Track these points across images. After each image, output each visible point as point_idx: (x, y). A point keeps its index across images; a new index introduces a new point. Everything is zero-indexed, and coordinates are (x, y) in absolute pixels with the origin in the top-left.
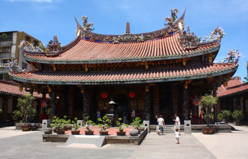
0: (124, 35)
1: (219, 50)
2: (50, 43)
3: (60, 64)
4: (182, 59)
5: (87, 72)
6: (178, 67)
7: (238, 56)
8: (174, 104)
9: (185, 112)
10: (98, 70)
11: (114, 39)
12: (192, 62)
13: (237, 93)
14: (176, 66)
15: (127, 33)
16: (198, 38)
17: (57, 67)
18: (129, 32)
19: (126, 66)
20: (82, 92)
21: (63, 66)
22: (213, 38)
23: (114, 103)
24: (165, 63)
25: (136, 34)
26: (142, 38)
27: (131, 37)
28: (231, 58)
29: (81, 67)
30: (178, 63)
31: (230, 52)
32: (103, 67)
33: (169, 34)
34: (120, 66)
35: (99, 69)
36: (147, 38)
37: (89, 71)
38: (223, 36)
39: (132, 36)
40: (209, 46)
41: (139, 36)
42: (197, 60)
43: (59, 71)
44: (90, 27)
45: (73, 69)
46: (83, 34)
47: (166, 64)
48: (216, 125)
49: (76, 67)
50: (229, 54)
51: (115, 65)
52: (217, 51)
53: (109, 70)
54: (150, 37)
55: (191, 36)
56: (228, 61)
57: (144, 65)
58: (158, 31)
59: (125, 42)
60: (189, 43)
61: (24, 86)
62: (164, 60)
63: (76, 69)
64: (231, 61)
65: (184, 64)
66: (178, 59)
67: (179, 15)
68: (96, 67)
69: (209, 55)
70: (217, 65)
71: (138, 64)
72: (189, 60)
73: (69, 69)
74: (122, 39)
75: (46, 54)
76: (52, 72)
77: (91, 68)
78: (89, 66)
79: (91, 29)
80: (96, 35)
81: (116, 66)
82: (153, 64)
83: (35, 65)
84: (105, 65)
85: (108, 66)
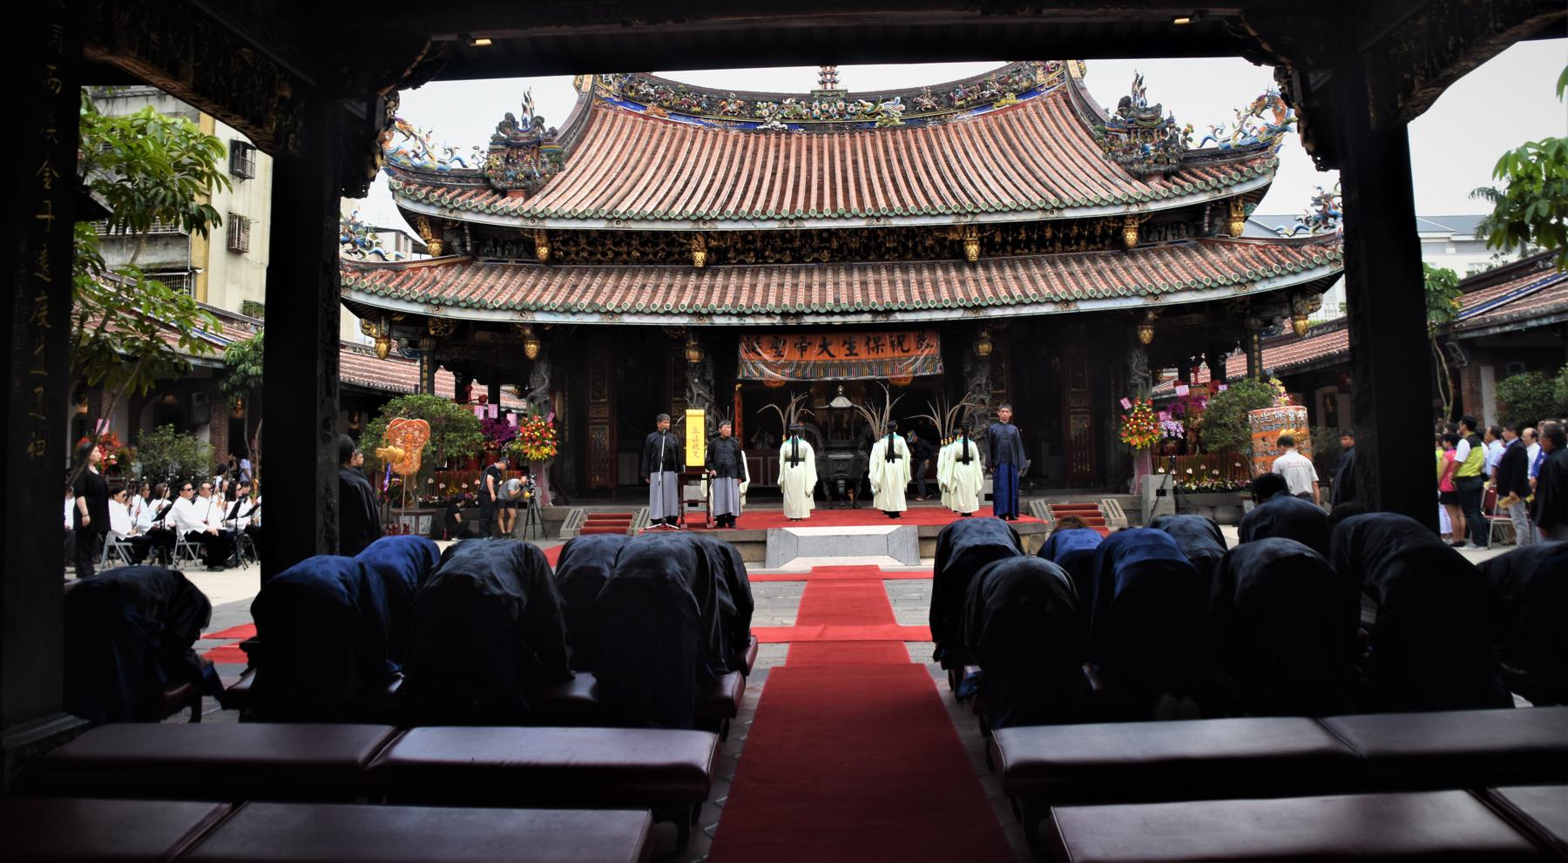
0: (809, 98)
2: (501, 127)
3: (566, 231)
4: (1121, 219)
5: (700, 268)
6: (1103, 253)
8: (1073, 413)
11: (765, 112)
12: (1160, 233)
13: (1314, 362)
14: (1092, 246)
15: (823, 83)
17: (551, 242)
20: (693, 355)
21: (583, 241)
24: (1049, 234)
25: (870, 93)
26: (895, 109)
27: (843, 104)
30: (1104, 235)
31: (1317, 194)
33: (1017, 97)
35: (752, 254)
36: (922, 112)
37: (707, 263)
39: (850, 98)
41: (883, 101)
42: (1178, 223)
43: (559, 261)
45: (629, 254)
47: (1054, 238)
49: (643, 244)
50: (1317, 201)
51: (828, 240)
54: (933, 109)
59: (815, 127)
60: (1144, 149)
61: (395, 334)
64: (1322, 231)
65: (1131, 237)
66: (1106, 218)
68: (739, 245)
70: (1265, 247)
71: (936, 234)
72: (1148, 224)
73: (611, 255)
74: (804, 111)
76: (521, 268)
78: (713, 243)
81: (835, 245)
82: (998, 239)
83: (443, 231)
84: (784, 240)
85: (797, 244)
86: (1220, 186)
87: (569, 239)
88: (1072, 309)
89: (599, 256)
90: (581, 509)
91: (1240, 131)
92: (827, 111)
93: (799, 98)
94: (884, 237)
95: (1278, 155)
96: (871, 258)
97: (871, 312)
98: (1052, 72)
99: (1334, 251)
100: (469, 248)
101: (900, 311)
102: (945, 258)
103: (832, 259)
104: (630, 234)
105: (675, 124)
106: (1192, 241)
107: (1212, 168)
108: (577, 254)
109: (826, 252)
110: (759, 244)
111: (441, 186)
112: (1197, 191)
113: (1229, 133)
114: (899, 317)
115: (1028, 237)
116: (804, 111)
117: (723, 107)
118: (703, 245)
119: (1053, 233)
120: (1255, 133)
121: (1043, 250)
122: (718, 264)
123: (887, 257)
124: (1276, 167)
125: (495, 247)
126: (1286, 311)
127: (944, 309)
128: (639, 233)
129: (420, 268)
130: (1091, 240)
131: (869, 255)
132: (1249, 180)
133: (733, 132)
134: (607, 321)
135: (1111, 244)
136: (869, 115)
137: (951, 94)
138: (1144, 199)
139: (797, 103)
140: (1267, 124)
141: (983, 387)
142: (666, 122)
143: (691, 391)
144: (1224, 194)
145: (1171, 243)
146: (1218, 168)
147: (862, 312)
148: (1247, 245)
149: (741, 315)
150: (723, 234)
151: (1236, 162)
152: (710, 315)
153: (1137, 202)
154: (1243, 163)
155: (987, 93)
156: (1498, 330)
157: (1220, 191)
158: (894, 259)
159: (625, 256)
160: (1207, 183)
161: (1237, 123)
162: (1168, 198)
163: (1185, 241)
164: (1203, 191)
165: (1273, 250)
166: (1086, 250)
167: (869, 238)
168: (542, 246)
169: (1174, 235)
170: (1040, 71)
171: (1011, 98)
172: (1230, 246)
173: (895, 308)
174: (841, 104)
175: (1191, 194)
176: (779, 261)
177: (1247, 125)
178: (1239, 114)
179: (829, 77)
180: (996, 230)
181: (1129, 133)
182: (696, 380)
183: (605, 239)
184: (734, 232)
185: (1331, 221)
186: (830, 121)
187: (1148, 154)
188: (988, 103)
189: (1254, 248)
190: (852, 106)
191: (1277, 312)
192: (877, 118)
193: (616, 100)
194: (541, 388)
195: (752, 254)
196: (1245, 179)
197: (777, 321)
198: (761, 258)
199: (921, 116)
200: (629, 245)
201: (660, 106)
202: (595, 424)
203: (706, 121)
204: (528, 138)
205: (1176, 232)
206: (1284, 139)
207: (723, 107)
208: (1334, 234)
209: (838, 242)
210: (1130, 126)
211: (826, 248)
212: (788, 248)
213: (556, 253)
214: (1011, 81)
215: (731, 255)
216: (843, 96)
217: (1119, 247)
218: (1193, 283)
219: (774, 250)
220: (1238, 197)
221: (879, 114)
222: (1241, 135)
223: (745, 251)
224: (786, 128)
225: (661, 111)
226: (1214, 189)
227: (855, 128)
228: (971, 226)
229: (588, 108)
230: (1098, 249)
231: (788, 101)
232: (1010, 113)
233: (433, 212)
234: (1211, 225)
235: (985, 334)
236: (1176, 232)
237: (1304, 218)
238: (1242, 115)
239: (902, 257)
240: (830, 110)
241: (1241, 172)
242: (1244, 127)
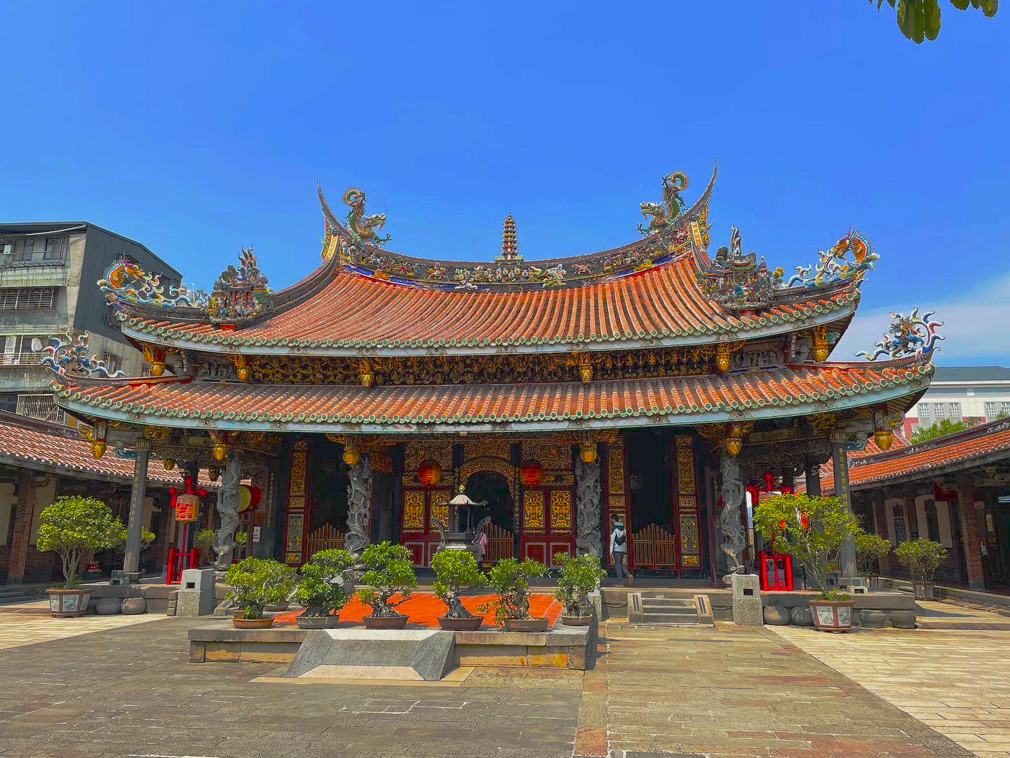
0: (495, 266)
1: (853, 315)
2: (224, 276)
3: (263, 357)
4: (716, 346)
5: (365, 388)
7: (932, 336)
9: (727, 539)
10: (408, 382)
12: (752, 360)
14: (691, 371)
15: (505, 255)
19: (512, 371)
20: (349, 458)
21: (276, 364)
22: (831, 271)
23: (471, 502)
24: (652, 361)
26: (558, 273)
28: (903, 343)
29: (347, 367)
30: (701, 362)
31: (897, 321)
32: (428, 373)
33: (653, 263)
36: (578, 275)
37: (374, 385)
39: (524, 266)
40: (816, 300)
43: (258, 381)
44: (375, 230)
45: (314, 376)
46: (347, 255)
47: (657, 364)
48: (852, 594)
49: (325, 368)
50: (896, 328)
51: (471, 366)
52: (847, 321)
53: (451, 381)
55: (746, 265)
56: (891, 355)
57: (577, 366)
58: (614, 253)
59: (500, 287)
60: (738, 290)
62: (649, 350)
63: (326, 377)
64: (904, 355)
65: (723, 362)
67: (689, 198)
69: (816, 334)
72: (740, 351)
75: (207, 316)
77: (384, 374)
79: (376, 238)
80: (398, 260)
81: (476, 369)
82: (609, 365)
84: (436, 366)
89: (291, 377)
92: (507, 276)
93: (486, 266)
96: (506, 380)
97: (490, 423)
99: (914, 372)
100: (185, 370)
102: (566, 381)
103: (474, 382)
104: (313, 359)
105: (395, 285)
111: (168, 320)
114: (515, 428)
118: (368, 368)
121: (649, 375)
122: (384, 384)
123: (519, 380)
124: (856, 301)
125: (210, 369)
128: (320, 359)
129: (140, 385)
130: (690, 364)
142: (388, 284)
144: (807, 325)
147: (483, 423)
148: (831, 369)
149: (384, 424)
150: (386, 359)
152: (358, 424)
155: (628, 260)
157: (803, 322)
159: (312, 378)
160: (791, 315)
163: (775, 367)
165: (855, 372)
168: (242, 368)
169: (765, 361)
171: (648, 264)
172: (815, 369)
173: (510, 420)
175: (777, 324)
176: (433, 382)
180: (607, 358)
182: (355, 479)
184: (394, 358)
185: (911, 345)
187: (742, 293)
193: (352, 267)
195: (411, 378)
197: (414, 429)
198: (418, 379)
201: (384, 272)
202: (293, 513)
204: (242, 284)
208: (914, 356)
211: (472, 372)
213: (256, 374)
217: (715, 371)
218: (775, 401)
220: (822, 327)
225: (384, 276)
227: (529, 288)
229: (329, 271)
230: (697, 374)
231: (478, 268)
233: (152, 339)
234: (798, 353)
235: (588, 444)
236: (766, 358)
237: (884, 343)
241: (824, 306)
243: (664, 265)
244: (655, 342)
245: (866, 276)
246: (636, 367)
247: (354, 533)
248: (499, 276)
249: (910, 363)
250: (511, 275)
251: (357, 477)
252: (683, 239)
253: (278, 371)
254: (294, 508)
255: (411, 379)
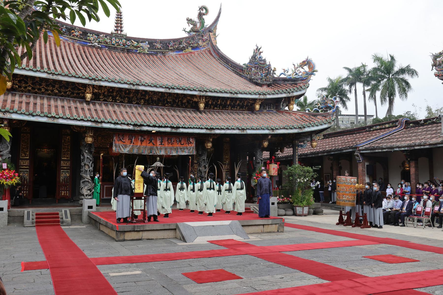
3: (22, 76)
4: (255, 100)
11: (92, 38)
14: (241, 109)
15: (117, 30)
16: (273, 69)
18: (122, 31)
24: (228, 103)
25: (136, 38)
26: (146, 46)
27: (125, 40)
30: (247, 106)
34: (155, 98)
36: (156, 49)
37: (91, 99)
38: (315, 72)
40: (291, 85)
41: (141, 42)
45: (52, 91)
51: (145, 96)
54: (160, 49)
58: (174, 40)
59: (112, 48)
65: (257, 107)
69: (291, 99)
71: (189, 98)
73: (43, 90)
78: (96, 91)
81: (147, 98)
82: (210, 103)
85: (132, 95)
86: (291, 92)
87: (23, 80)
88: (245, 132)
90: (31, 210)
91: (295, 72)
92: (118, 43)
93: (106, 35)
94: (167, 97)
95: (309, 83)
96: (160, 105)
97: (171, 127)
98: (205, 42)
101: (182, 128)
102: (188, 108)
106: (275, 111)
107: (284, 85)
108: (25, 87)
109: (142, 100)
110: (115, 94)
112: (283, 92)
113: (290, 72)
115: (221, 103)
116: (108, 41)
117: (73, 33)
119: (230, 102)
120: (300, 74)
121: (224, 109)
123: (166, 105)
124: (308, 87)
126: (309, 139)
127: (199, 128)
128: (61, 82)
131: (159, 103)
132: (299, 91)
133: (77, 45)
134: (50, 121)
135: (247, 109)
136: (135, 47)
137: (168, 44)
138: (266, 93)
139: (106, 37)
140: (306, 71)
141: (205, 160)
143: (83, 155)
145: (268, 111)
146: (286, 85)
147: (167, 127)
150: (100, 87)
151: (293, 84)
153: (264, 94)
154: (296, 84)
156: (380, 151)
157: (290, 94)
158: (168, 106)
160: (286, 90)
161: (294, 70)
162: (273, 94)
163: (272, 111)
164: (285, 93)
166: (239, 110)
167: (161, 97)
168: (9, 81)
169: (269, 108)
170: (200, 41)
171: (190, 48)
174: (124, 41)
177: (298, 71)
178: (295, 66)
179: (119, 28)
180: (211, 99)
181: (255, 68)
182: (87, 151)
183: (43, 82)
184: (106, 87)
186: (119, 47)
188: (182, 50)
189: (299, 116)
190: (128, 42)
191: (305, 139)
192: (139, 49)
194: (7, 151)
196: (299, 90)
197: (131, 127)
198: (114, 100)
199: (155, 51)
200: (54, 86)
203: (64, 38)
205: (269, 107)
206: (311, 78)
207: (73, 33)
209: (148, 96)
210: (256, 65)
211: (143, 99)
212: (127, 97)
214: (191, 42)
215: (101, 97)
216: (125, 37)
219: (120, 97)
220: (294, 97)
221: (139, 47)
222: (295, 74)
223: (108, 96)
224: (100, 46)
226: (289, 92)
227: (129, 51)
228: (203, 96)
230: (243, 110)
231: (102, 35)
232: (189, 55)
238: (296, 66)
239: (172, 106)
240: (119, 42)
242: (297, 72)
243: (197, 52)
244: (235, 95)
245: (312, 77)
246: (221, 104)
247: (86, 180)
248: (114, 42)
249: (328, 116)
250: (121, 43)
251: (88, 150)
252: (206, 40)
253: (30, 85)
254: (23, 166)
255: (110, 99)
